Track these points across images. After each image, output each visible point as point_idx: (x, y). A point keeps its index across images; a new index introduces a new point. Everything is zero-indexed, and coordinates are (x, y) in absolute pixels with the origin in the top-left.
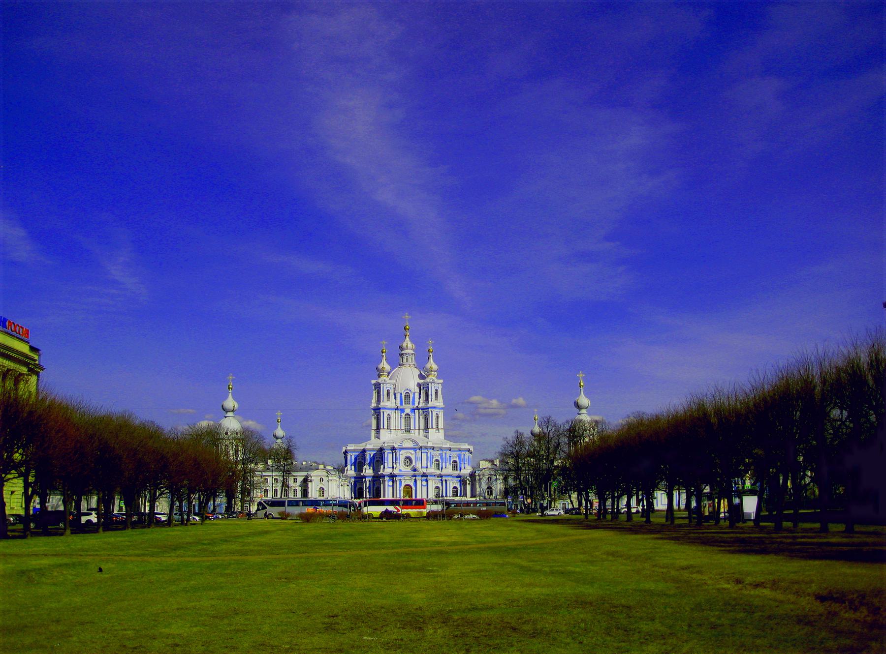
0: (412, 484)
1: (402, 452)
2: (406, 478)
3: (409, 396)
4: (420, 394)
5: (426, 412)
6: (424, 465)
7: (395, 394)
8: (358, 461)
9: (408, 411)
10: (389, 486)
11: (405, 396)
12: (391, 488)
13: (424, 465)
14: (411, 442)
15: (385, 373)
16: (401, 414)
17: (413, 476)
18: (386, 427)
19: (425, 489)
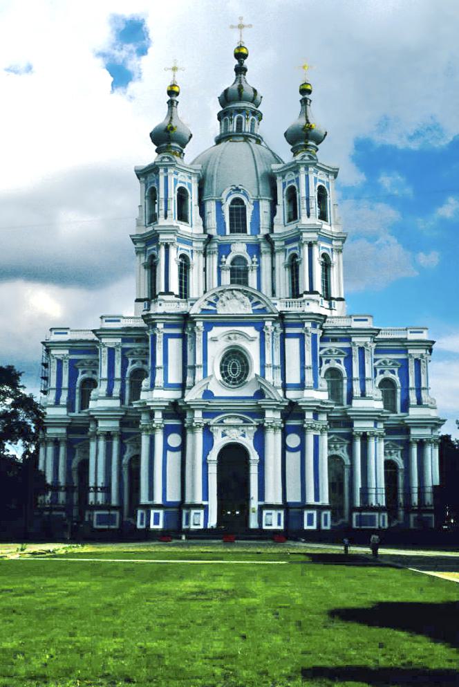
0: (248, 442)
1: (216, 332)
2: (227, 421)
3: (244, 209)
4: (274, 203)
5: (295, 248)
6: (293, 377)
7: (201, 204)
8: (80, 377)
9: (239, 249)
10: (167, 447)
11: (231, 209)
12: (174, 458)
13: (293, 377)
14: (247, 300)
15: (173, 144)
16: (220, 257)
17: (253, 415)
18: (174, 287)
19: (293, 459)
